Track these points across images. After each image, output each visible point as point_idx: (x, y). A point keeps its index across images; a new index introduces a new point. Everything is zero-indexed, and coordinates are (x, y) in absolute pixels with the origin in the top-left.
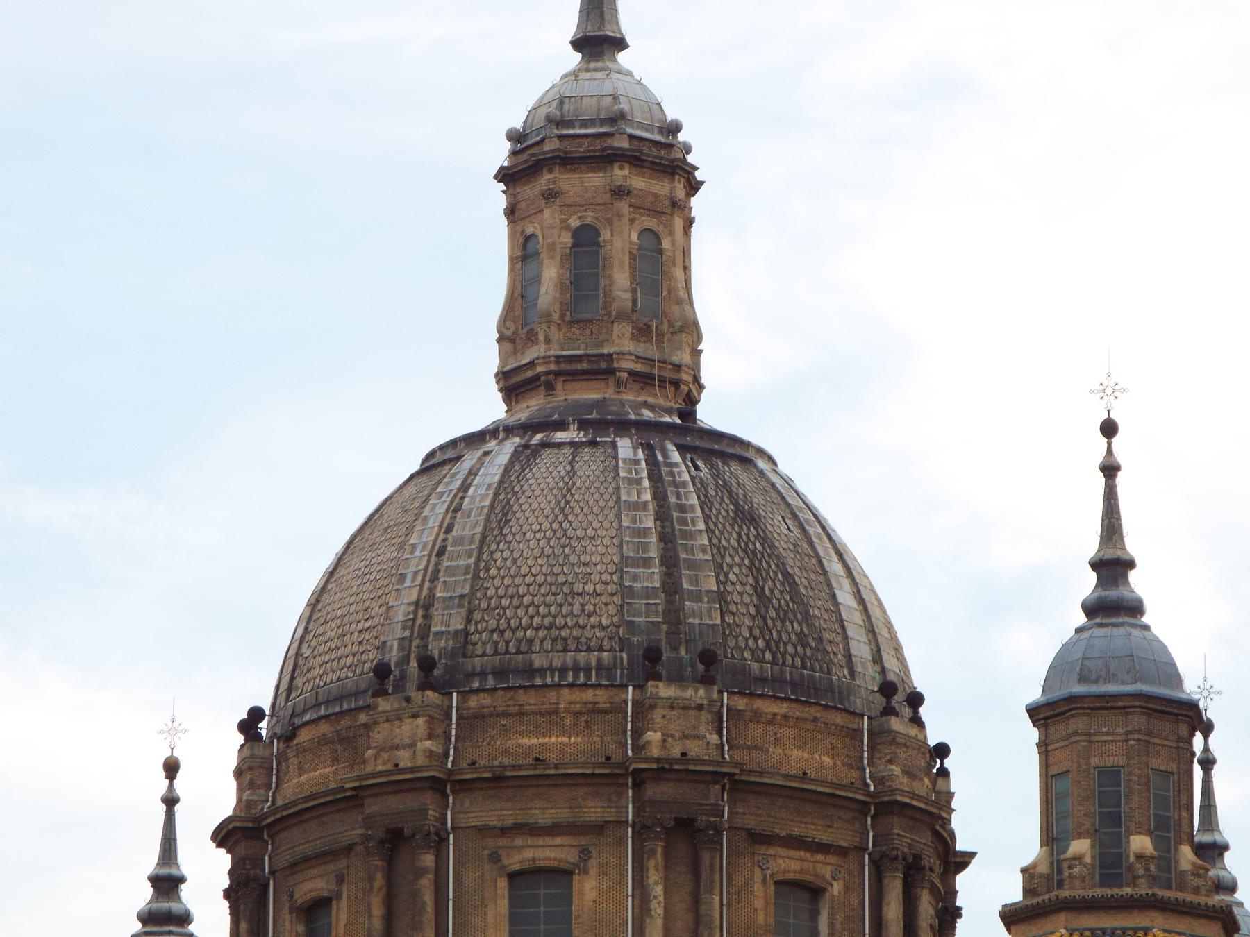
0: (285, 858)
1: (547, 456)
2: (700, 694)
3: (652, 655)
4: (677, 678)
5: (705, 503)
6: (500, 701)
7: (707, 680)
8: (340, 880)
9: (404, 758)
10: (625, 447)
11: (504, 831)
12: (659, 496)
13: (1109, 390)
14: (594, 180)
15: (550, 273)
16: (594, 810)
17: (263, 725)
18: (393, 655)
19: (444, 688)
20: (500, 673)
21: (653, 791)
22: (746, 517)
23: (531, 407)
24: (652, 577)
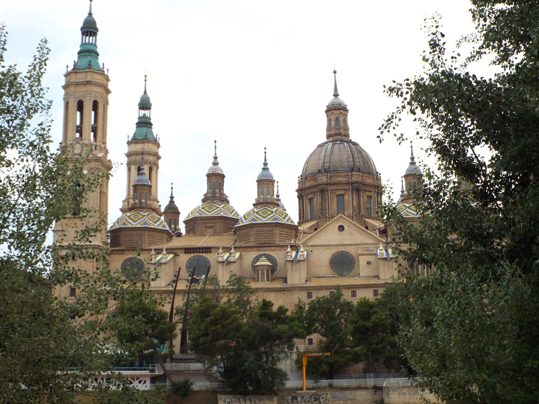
0: (306, 193)
2: (358, 173)
3: (353, 169)
4: (355, 171)
6: (334, 174)
7: (359, 172)
9: (323, 181)
10: (345, 144)
14: (338, 112)
15: (333, 123)
16: (346, 187)
19: (327, 173)
20: (334, 171)
21: (354, 185)
22: (360, 152)
23: (331, 139)
24: (351, 159)
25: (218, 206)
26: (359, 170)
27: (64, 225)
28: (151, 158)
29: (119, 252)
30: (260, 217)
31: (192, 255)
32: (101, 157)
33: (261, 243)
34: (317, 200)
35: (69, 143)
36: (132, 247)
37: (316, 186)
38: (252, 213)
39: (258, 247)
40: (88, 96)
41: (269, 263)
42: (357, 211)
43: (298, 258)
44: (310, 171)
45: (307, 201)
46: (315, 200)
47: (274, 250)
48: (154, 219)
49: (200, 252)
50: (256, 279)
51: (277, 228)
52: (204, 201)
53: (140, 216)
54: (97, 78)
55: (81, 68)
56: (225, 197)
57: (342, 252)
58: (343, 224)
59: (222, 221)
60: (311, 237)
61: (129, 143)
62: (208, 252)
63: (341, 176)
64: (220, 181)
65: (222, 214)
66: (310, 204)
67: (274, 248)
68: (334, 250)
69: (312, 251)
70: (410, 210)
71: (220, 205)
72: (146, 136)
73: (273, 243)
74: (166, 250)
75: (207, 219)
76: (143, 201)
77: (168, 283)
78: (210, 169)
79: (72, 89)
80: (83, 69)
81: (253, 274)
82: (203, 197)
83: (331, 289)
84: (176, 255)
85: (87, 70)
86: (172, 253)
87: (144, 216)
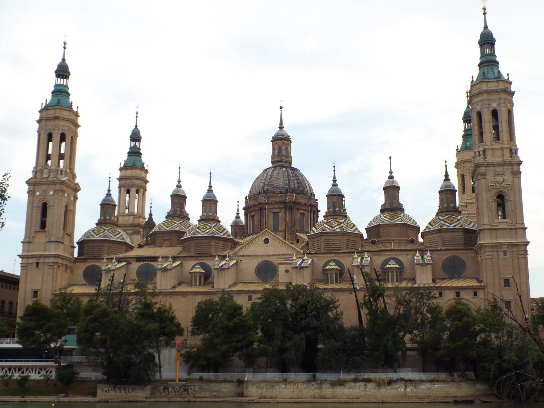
1: (276, 170)
3: (287, 190)
4: (290, 193)
5: (292, 175)
7: (293, 193)
8: (255, 213)
9: (262, 201)
10: (284, 169)
11: (272, 208)
12: (288, 174)
13: (334, 163)
14: (281, 142)
15: (276, 151)
16: (281, 206)
17: (247, 198)
18: (261, 191)
20: (272, 192)
21: (287, 204)
22: (297, 176)
23: (274, 165)
24: (287, 182)
25: (176, 222)
26: (293, 191)
27: (31, 238)
28: (138, 182)
29: (82, 260)
30: (200, 231)
31: (142, 263)
32: (64, 181)
33: (199, 254)
34: (257, 218)
35: (39, 168)
36: (93, 256)
38: (195, 227)
40: (56, 129)
41: (202, 271)
42: (290, 226)
43: (363, 263)
44: (254, 192)
45: (251, 218)
46: (256, 217)
47: (210, 260)
48: (115, 232)
49: (148, 261)
50: (325, 281)
51: (213, 241)
52: (167, 217)
53: (103, 230)
54: (65, 114)
55: (51, 106)
56: (185, 214)
57: (267, 261)
58: (265, 238)
59: (177, 234)
60: (241, 249)
61: (121, 169)
62: (155, 261)
64: (181, 201)
65: (178, 229)
66: (253, 221)
67: (209, 258)
68: (260, 260)
69: (241, 261)
70: (326, 226)
71: (178, 221)
72: (134, 163)
73: (209, 254)
74: (116, 258)
75: (164, 233)
76: (108, 217)
77: (173, 285)
78: (174, 191)
79: (43, 123)
80: (53, 106)
81: (323, 277)
82: (167, 214)
83: (250, 293)
84: (129, 263)
85: (55, 107)
86: (126, 261)
87: (106, 230)
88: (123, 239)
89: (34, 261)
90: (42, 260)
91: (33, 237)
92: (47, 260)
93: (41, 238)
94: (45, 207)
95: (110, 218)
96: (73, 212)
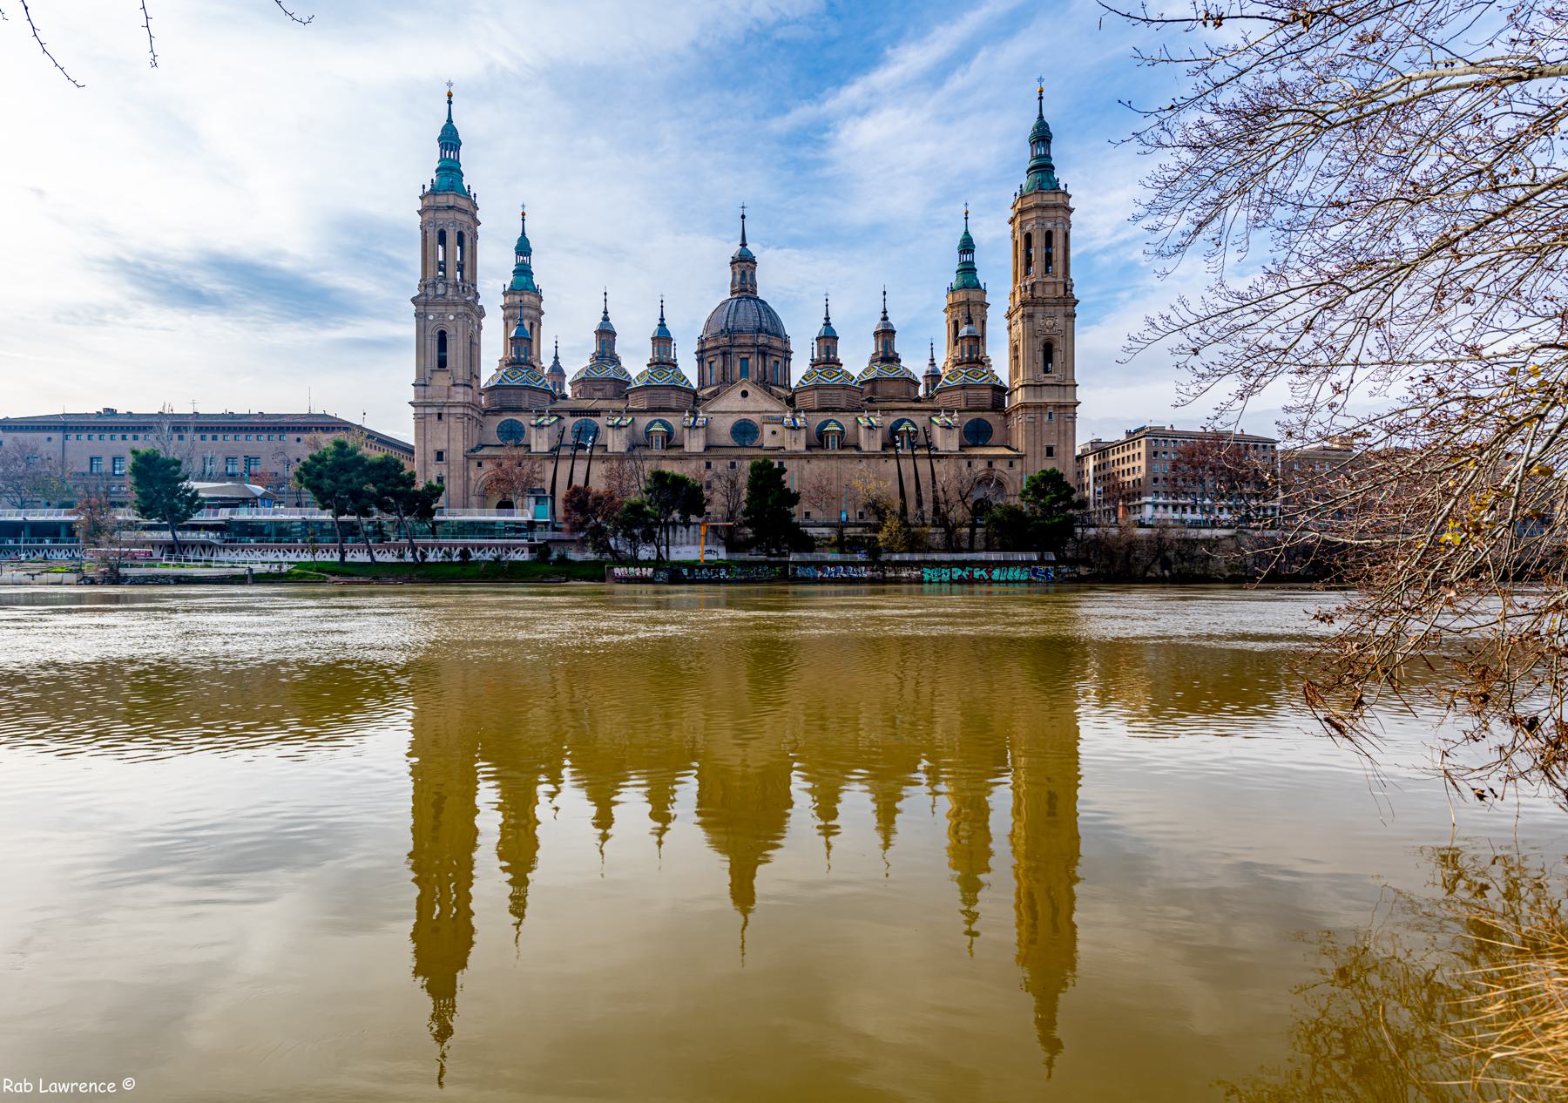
13: (827, 295)
15: (738, 277)
31: (579, 418)
37: (716, 348)
39: (652, 410)
45: (707, 365)
54: (462, 203)
63: (745, 337)
65: (613, 376)
68: (736, 418)
84: (560, 418)
88: (547, 385)
89: (435, 410)
90: (445, 411)
91: (430, 378)
92: (453, 410)
93: (442, 379)
94: (442, 338)
95: (526, 358)
96: (479, 345)
